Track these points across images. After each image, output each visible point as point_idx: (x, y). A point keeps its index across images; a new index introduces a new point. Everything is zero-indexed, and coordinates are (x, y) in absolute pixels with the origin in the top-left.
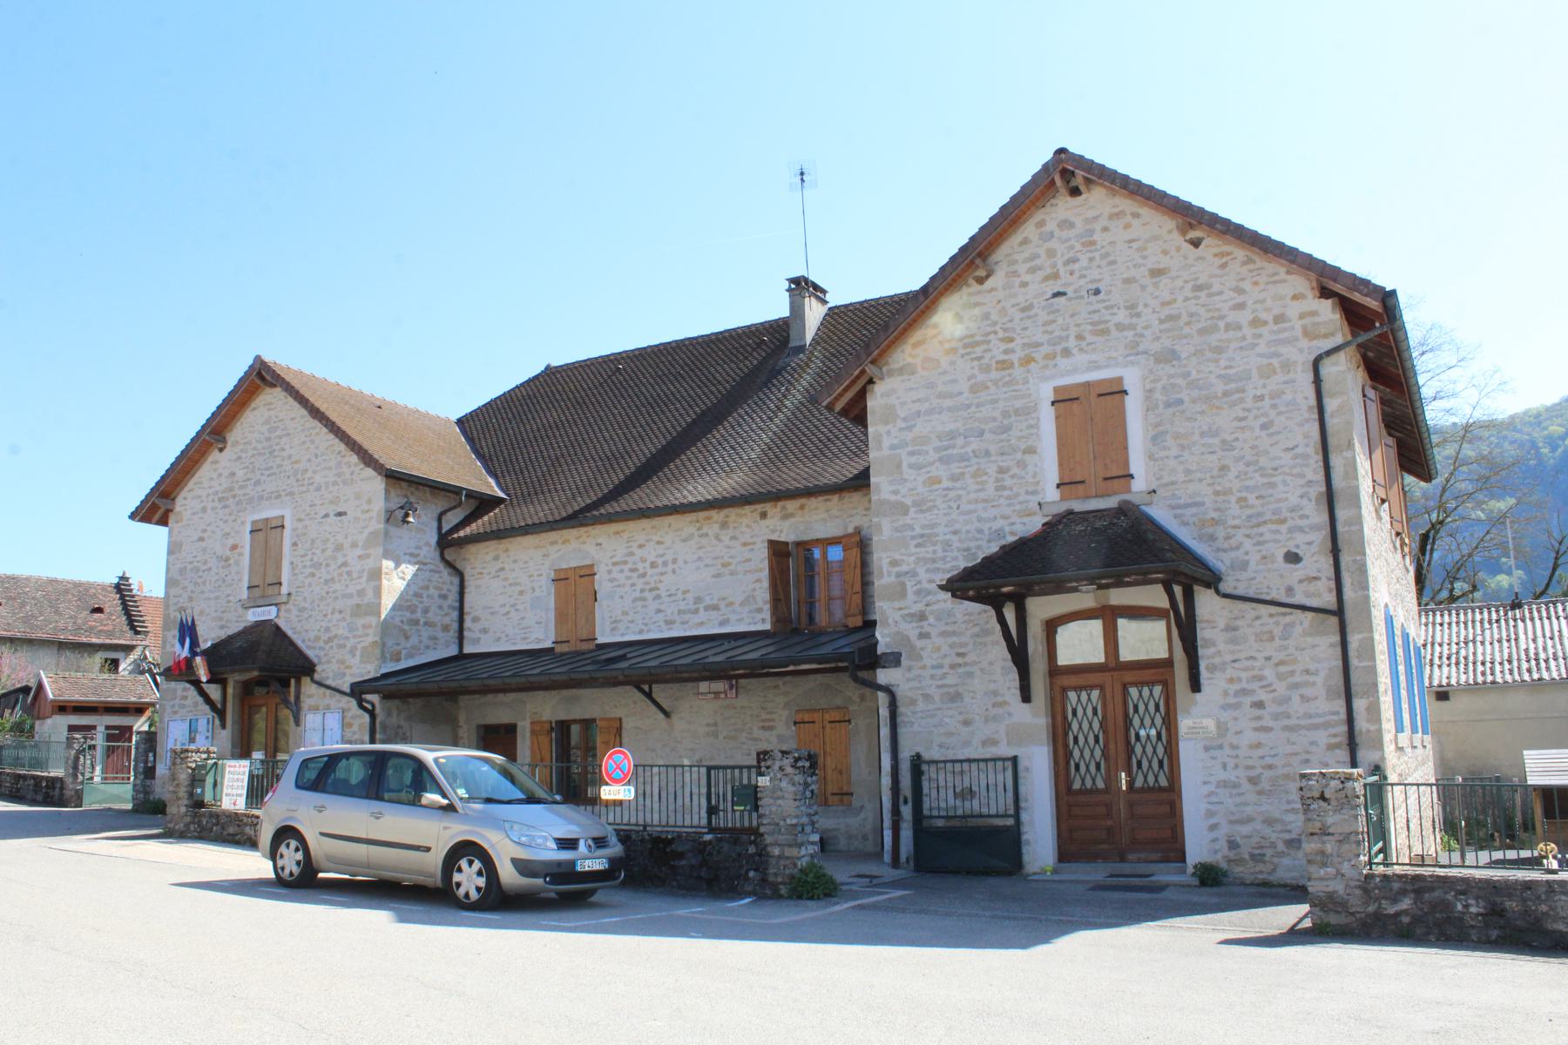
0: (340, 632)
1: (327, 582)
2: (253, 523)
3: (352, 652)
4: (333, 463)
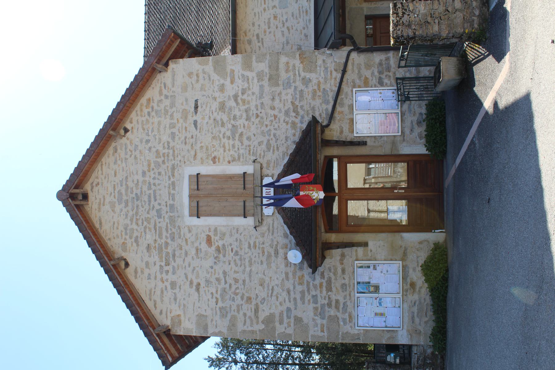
0: (289, 98)
2: (191, 215)
3: (306, 82)
4: (156, 120)
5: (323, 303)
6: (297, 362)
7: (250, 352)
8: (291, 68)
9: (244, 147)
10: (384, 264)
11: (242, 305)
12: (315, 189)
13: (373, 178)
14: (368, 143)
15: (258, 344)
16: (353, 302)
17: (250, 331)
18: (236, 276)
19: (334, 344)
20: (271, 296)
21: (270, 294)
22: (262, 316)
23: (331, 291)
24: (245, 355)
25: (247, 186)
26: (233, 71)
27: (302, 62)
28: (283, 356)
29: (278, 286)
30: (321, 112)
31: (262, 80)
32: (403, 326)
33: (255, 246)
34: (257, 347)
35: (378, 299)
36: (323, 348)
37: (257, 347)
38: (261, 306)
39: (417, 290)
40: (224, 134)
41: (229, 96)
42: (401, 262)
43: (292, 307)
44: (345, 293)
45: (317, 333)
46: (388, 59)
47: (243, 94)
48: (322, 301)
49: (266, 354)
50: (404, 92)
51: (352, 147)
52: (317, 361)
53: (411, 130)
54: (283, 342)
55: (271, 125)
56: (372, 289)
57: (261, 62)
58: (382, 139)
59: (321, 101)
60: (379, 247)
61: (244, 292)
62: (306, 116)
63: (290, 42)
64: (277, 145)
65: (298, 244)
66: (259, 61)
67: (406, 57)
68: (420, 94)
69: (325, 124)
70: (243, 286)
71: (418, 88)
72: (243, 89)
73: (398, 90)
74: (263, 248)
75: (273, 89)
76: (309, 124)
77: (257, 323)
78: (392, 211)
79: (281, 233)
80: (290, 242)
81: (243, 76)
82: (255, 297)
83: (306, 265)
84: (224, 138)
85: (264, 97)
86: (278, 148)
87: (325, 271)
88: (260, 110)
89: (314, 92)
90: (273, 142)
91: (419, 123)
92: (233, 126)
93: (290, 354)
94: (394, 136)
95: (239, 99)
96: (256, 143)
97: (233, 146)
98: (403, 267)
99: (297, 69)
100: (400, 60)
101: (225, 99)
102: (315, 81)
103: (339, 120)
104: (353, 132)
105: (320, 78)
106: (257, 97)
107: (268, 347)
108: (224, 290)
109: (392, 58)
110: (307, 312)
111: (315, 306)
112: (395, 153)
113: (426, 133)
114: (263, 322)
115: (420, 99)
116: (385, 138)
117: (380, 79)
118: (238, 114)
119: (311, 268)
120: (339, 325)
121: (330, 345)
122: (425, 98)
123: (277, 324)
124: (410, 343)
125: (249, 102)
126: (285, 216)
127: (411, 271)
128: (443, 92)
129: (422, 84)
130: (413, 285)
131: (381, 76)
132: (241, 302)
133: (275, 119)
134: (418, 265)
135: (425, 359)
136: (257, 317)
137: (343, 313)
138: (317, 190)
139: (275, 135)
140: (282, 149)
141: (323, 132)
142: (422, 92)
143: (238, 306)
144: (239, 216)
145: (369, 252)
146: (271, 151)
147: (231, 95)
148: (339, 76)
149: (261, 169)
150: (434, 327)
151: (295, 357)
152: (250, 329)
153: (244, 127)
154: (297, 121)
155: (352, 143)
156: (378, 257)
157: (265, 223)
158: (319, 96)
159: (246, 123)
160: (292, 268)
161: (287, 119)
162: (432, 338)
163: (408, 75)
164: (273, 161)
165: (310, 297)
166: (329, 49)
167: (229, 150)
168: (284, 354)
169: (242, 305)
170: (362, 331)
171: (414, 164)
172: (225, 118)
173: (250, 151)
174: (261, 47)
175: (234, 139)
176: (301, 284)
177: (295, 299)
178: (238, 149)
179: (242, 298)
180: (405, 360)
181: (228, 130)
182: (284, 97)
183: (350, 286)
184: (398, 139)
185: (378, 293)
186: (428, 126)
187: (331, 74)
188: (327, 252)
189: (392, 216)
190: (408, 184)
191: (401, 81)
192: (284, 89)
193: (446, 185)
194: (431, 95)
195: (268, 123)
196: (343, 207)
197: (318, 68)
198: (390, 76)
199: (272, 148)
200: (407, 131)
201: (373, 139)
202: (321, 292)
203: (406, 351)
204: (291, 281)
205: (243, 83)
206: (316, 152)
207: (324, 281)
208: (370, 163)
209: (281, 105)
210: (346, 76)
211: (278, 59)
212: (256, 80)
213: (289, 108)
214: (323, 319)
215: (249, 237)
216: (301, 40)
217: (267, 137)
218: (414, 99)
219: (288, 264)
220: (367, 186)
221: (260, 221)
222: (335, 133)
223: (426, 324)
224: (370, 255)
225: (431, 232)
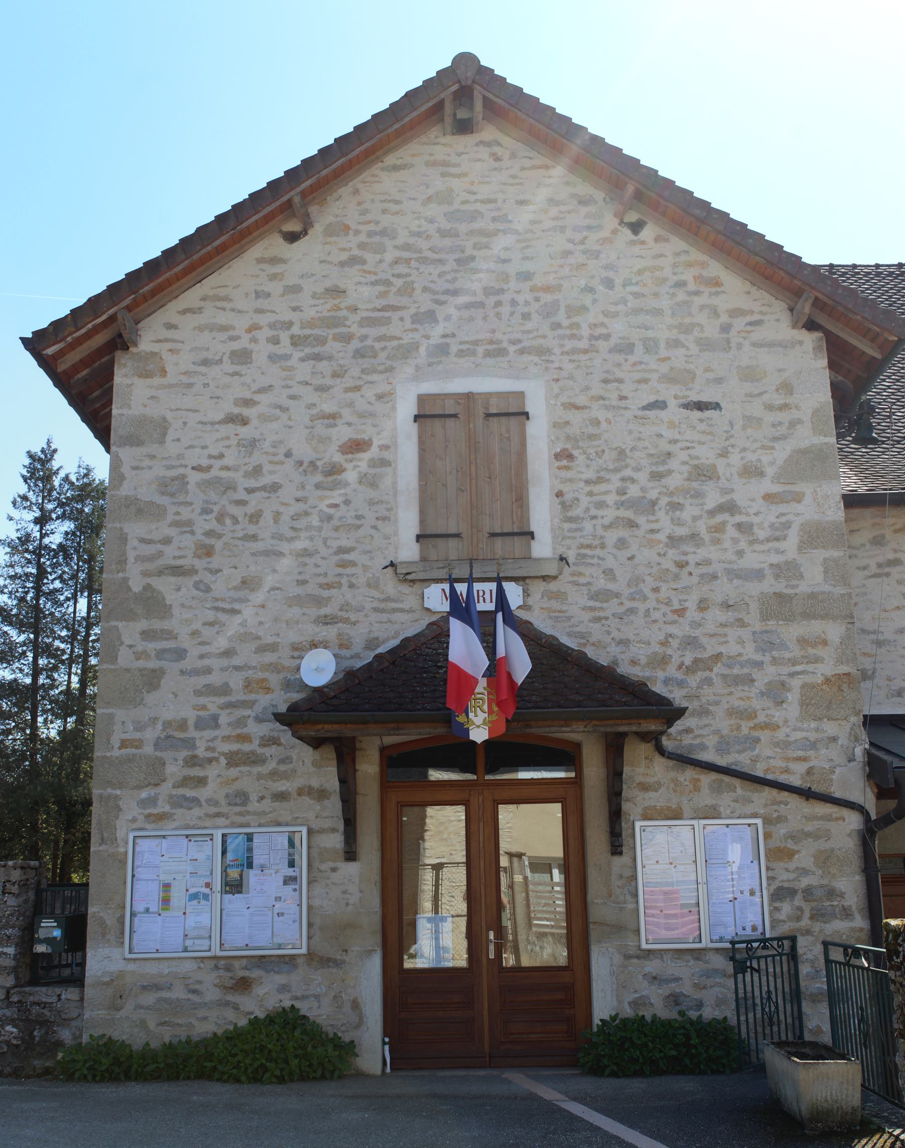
0: (732, 649)
1: (673, 541)
2: (422, 399)
3: (776, 692)
4: (665, 303)
5: (198, 743)
6: (42, 680)
7: (67, 556)
8: (811, 651)
9: (600, 531)
10: (300, 905)
11: (192, 533)
12: (494, 717)
13: (526, 878)
14: (617, 861)
15: (90, 577)
16: (201, 824)
17: (124, 553)
18: (268, 516)
19: (89, 776)
20: (217, 609)
21: (220, 604)
22: (165, 586)
23: (230, 765)
24: (60, 545)
25: (499, 542)
26: (798, 498)
27: (827, 680)
28: (57, 643)
29: (241, 624)
30: (697, 732)
31: (777, 577)
32: (135, 960)
33: (343, 564)
34: (82, 576)
35: (207, 891)
36: (76, 748)
37: (82, 576)
38: (189, 582)
39: (230, 998)
40: (633, 480)
41: (732, 490)
42: (304, 951)
43: (186, 664)
44: (223, 802)
45: (119, 729)
46: (846, 913)
47: (739, 526)
48: (202, 741)
49: (62, 598)
50: (758, 958)
51: (607, 815)
52: (43, 733)
53: (655, 978)
54: (94, 641)
55: (658, 601)
56: (234, 874)
57: (826, 572)
58: (629, 897)
59: (725, 732)
60: (344, 892)
61: (225, 539)
62: (684, 692)
63: (883, 650)
64: (607, 618)
65: (350, 674)
66: (831, 569)
67: (854, 961)
68: (754, 1005)
69: (665, 742)
70: (241, 534)
71: (769, 998)
72: (751, 526)
73: (764, 941)
74: (340, 585)
75: (754, 606)
76: (662, 701)
77: (145, 574)
78: (437, 926)
79: (379, 631)
80: (357, 656)
81: (787, 525)
82: (214, 565)
83: (296, 696)
84: (623, 479)
85: (731, 580)
86: (598, 619)
87: (280, 748)
88: (697, 571)
89: (750, 715)
90: (613, 607)
91: (675, 999)
92: (654, 503)
93: (63, 662)
94: (638, 931)
95: (726, 516)
96: (610, 563)
97: (601, 505)
98: (293, 957)
99: (810, 667)
100: (845, 948)
101: (723, 480)
102: (778, 715)
103: (675, 781)
104: (646, 818)
105: (788, 730)
106: (730, 562)
107: (83, 604)
108: (231, 487)
109: (852, 926)
110: (173, 702)
111: (191, 723)
112: (594, 935)
113: (648, 1018)
114: (148, 587)
115: (742, 1002)
116: (631, 906)
117: (792, 892)
118: (686, 515)
119: (289, 709)
120: (139, 787)
121: (85, 766)
122: (743, 1018)
123: (142, 624)
124: (88, 981)
125: (716, 542)
126: (423, 640)
127: (280, 979)
128: (761, 1069)
129: (781, 1008)
130: (243, 985)
131: (799, 896)
132: (199, 532)
133: (675, 612)
134: (297, 998)
135: (45, 1023)
136: (160, 573)
137: (171, 796)
138: (492, 722)
139: (632, 611)
140: (596, 632)
141: (644, 737)
142: (759, 1008)
143: (189, 523)
144: (422, 522)
145: (332, 864)
146: (591, 603)
147: (734, 496)
148: (795, 781)
149: (544, 578)
150: (130, 1046)
151: (56, 675)
152: (131, 555)
153: (652, 531)
154: (672, 671)
155: (615, 815)
156: (318, 889)
157: (405, 589)
158: (739, 728)
159: (662, 537)
160: (287, 663)
161: (675, 643)
162: (101, 1043)
163: (804, 969)
164: (565, 608)
165: (213, 709)
166: (868, 753)
167: (590, 494)
168: (62, 646)
169: (192, 533)
170: (122, 850)
171: (568, 985)
172: (674, 481)
173: (589, 546)
174: (867, 573)
175: (620, 505)
176: (248, 685)
177: (208, 671)
178: (594, 517)
179: (209, 533)
180: (43, 968)
181: (643, 489)
182: (733, 634)
183: (240, 814)
184: (631, 943)
185: (224, 892)
186: (669, 1023)
187: (799, 759)
188: (329, 752)
189: (424, 928)
190: (512, 969)
191: (787, 948)
192: (754, 633)
193: (509, 1075)
194: (752, 1035)
195: (664, 593)
196: (445, 795)
197: (813, 725)
198: (798, 919)
199: (598, 604)
200: (652, 966)
201: (628, 873)
202: (226, 739)
203: (66, 972)
204: (255, 660)
205: (766, 525)
206: (588, 722)
207: (253, 746)
208: (566, 869)
209: (711, 628)
210: (795, 801)
211: (834, 618)
212: (775, 559)
213: (705, 649)
214: (157, 745)
215: (369, 548)
216: (889, 679)
217: (626, 592)
218: (741, 985)
219: (300, 650)
220: (504, 862)
221: (409, 577)
222: (641, 770)
223: (137, 1026)
224: (324, 867)
225: (385, 1035)
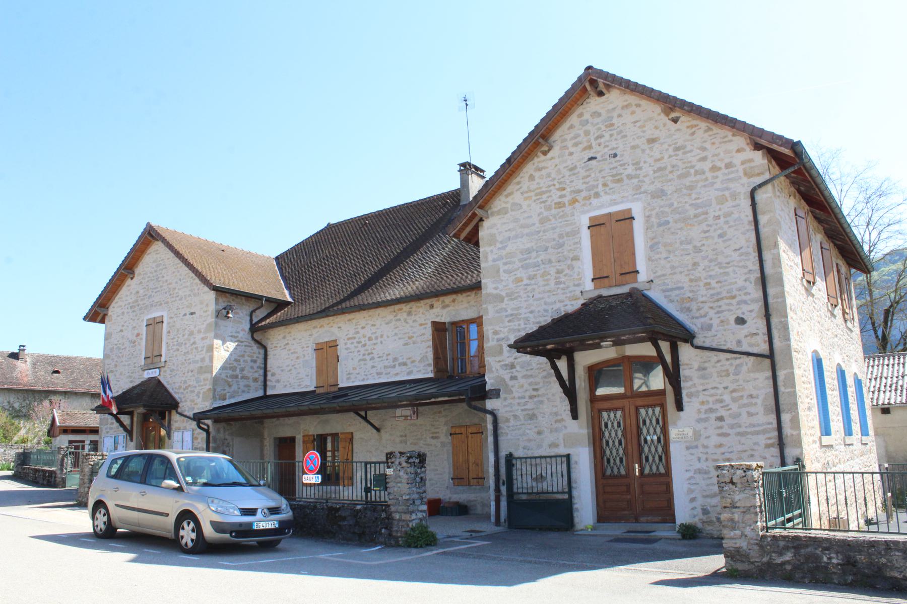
1: (185, 354)
4: (188, 284)
